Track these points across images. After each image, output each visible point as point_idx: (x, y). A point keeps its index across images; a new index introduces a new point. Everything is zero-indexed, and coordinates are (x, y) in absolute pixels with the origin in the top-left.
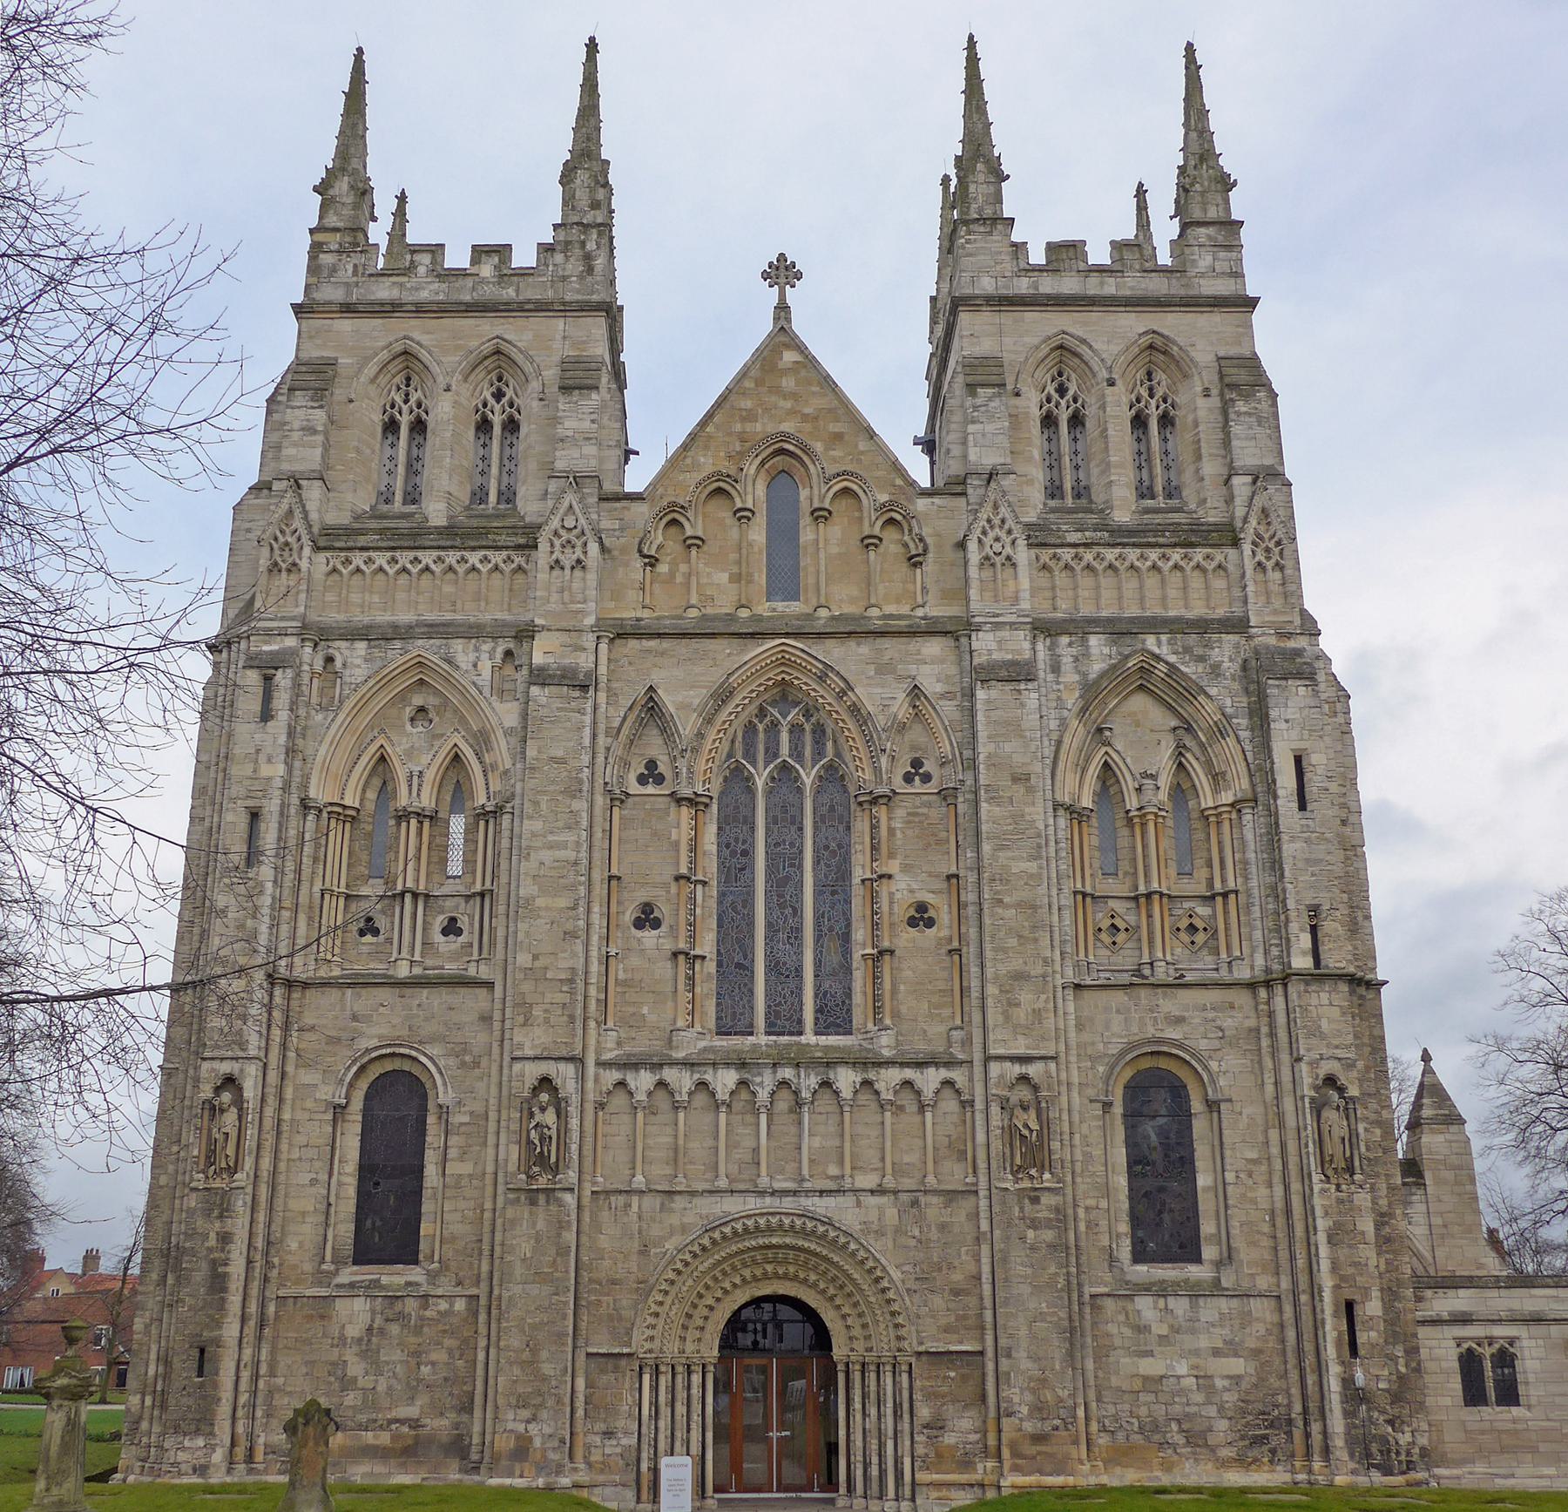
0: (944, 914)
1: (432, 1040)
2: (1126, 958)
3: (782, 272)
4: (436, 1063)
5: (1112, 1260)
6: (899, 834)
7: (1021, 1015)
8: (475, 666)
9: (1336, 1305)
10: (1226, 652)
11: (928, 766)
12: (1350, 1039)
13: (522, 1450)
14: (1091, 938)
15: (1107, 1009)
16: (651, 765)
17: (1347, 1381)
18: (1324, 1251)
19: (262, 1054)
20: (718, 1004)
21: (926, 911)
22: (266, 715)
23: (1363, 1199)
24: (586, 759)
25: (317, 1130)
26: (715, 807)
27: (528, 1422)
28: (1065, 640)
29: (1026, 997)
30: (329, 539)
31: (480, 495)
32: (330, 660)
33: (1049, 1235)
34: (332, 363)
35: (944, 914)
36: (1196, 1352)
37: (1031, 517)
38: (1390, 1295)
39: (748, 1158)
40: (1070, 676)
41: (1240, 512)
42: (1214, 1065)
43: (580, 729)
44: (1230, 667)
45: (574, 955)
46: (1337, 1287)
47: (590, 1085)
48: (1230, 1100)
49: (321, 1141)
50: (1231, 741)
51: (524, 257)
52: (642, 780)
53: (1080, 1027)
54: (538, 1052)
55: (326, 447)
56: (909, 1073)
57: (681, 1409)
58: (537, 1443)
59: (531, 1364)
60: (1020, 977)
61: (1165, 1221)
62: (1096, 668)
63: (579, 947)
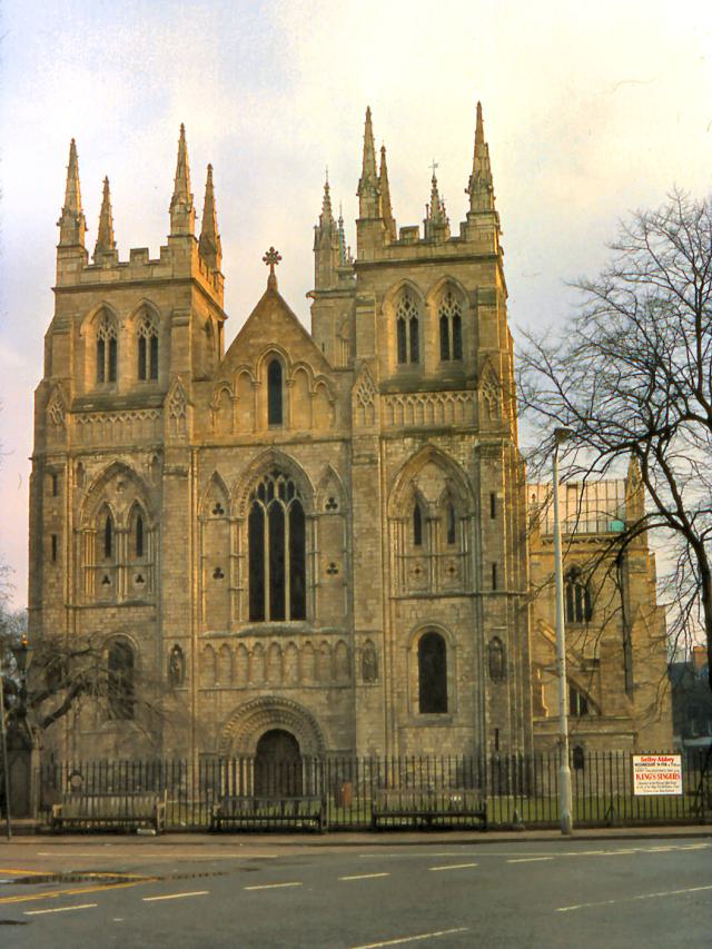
3: (272, 258)
4: (137, 641)
5: (410, 713)
16: (218, 505)
26: (247, 522)
32: (80, 464)
35: (340, 567)
51: (155, 255)
61: (434, 697)
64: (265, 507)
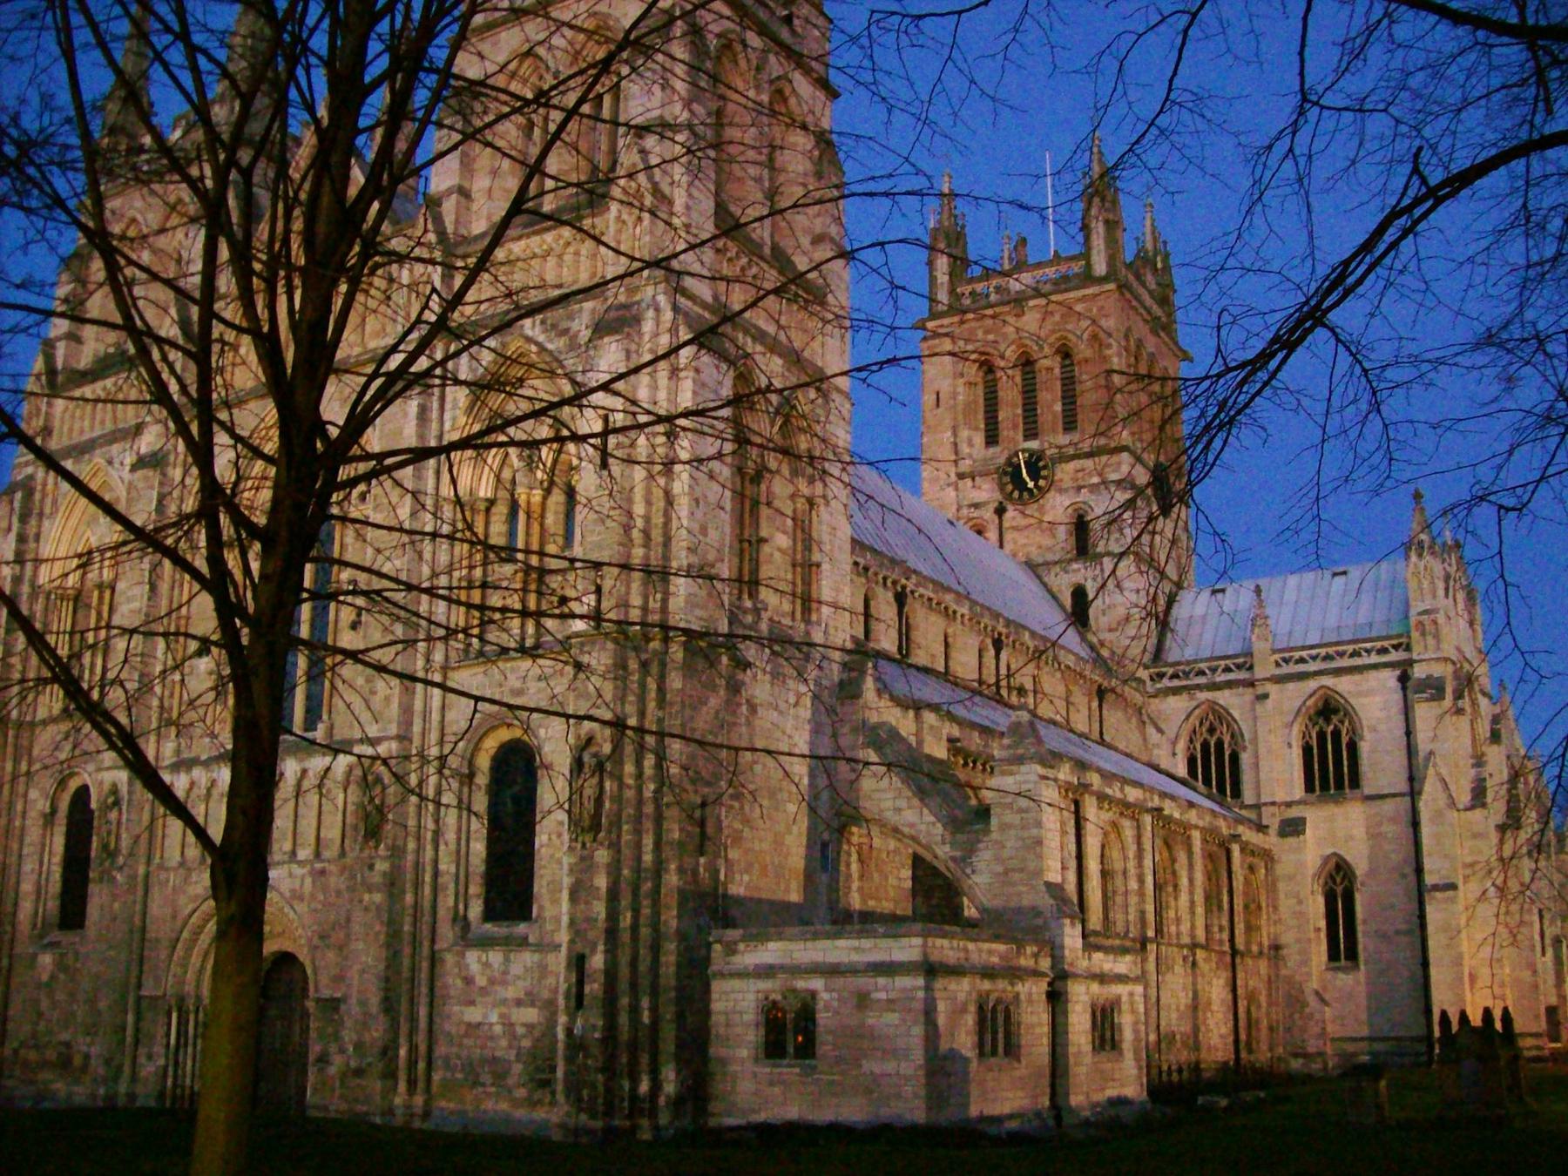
36: (504, 1002)
46: (572, 942)
59: (92, 1002)
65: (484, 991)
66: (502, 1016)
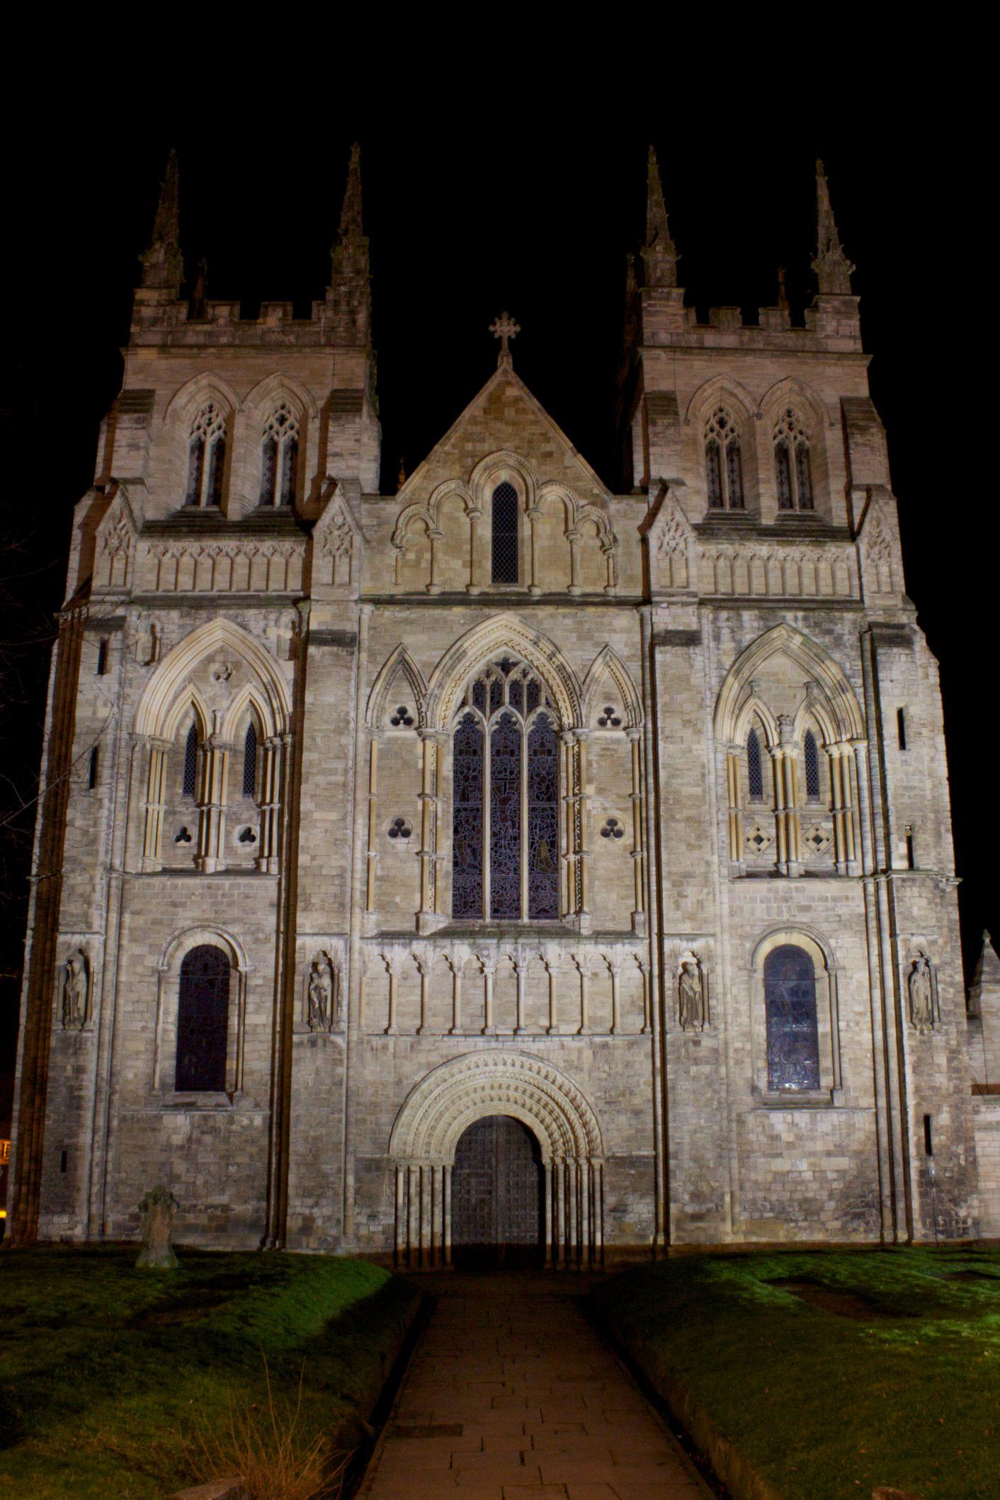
0: (629, 830)
1: (234, 921)
2: (768, 860)
6: (595, 765)
7: (689, 904)
8: (264, 631)
9: (917, 1116)
10: (847, 624)
11: (619, 713)
12: (933, 922)
13: (307, 1227)
14: (741, 846)
15: (753, 900)
16: (402, 711)
17: (923, 1173)
18: (909, 1078)
19: (103, 931)
20: (454, 895)
21: (616, 824)
22: (102, 669)
23: (938, 1040)
24: (352, 704)
25: (146, 991)
27: (312, 1207)
28: (724, 615)
29: (692, 891)
30: (152, 529)
31: (268, 498)
33: (706, 1069)
34: (150, 393)
36: (813, 1154)
37: (698, 519)
38: (957, 1108)
39: (479, 1011)
40: (728, 645)
41: (857, 520)
42: (832, 942)
43: (348, 680)
44: (850, 639)
45: (344, 856)
46: (918, 1105)
47: (356, 956)
48: (844, 968)
49: (149, 998)
50: (849, 695)
52: (395, 722)
53: (732, 914)
54: (316, 931)
55: (147, 458)
56: (603, 949)
57: (427, 1199)
58: (319, 1222)
60: (688, 875)
62: (748, 637)
63: (347, 850)
64: (488, 725)
65: (790, 1145)
66: (812, 1165)
